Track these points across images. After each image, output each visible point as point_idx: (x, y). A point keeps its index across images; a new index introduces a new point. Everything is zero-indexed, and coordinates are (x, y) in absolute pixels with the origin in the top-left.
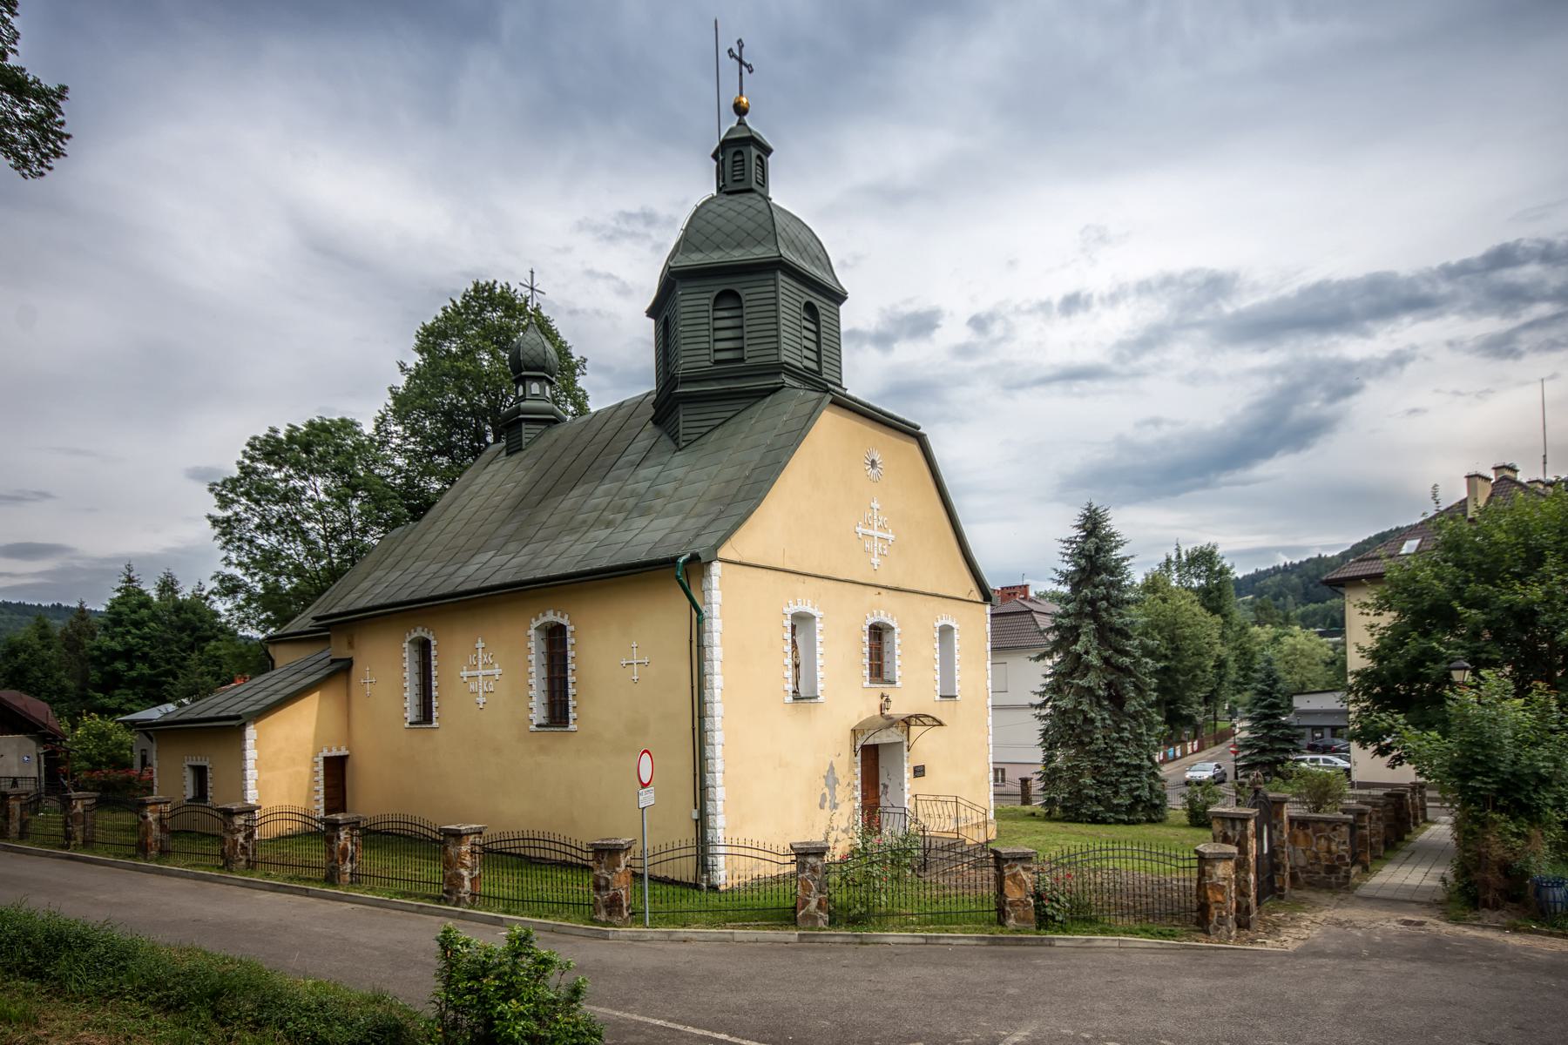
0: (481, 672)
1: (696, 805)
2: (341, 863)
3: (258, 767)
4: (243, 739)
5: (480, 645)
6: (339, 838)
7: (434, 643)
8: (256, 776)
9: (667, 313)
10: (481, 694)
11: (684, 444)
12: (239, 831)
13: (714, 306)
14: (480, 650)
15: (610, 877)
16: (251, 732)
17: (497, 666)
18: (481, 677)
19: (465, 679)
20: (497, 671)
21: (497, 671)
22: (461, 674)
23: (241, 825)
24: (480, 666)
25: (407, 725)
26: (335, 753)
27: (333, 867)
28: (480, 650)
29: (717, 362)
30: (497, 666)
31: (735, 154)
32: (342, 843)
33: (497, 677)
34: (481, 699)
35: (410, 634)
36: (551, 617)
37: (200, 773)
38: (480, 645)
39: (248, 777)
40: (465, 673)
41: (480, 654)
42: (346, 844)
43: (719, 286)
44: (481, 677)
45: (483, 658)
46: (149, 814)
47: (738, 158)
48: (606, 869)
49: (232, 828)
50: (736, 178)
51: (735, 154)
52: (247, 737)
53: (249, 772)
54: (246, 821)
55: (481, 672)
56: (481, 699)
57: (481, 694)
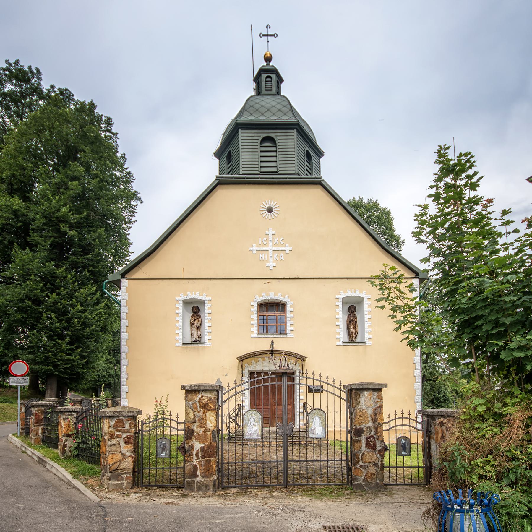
10: (271, 260)
13: (261, 144)
14: (271, 236)
18: (271, 251)
22: (251, 249)
24: (271, 244)
28: (271, 236)
29: (262, 173)
30: (287, 245)
31: (267, 77)
33: (287, 251)
43: (264, 133)
44: (271, 251)
47: (269, 79)
50: (267, 89)
51: (267, 77)
55: (271, 247)
57: (271, 260)
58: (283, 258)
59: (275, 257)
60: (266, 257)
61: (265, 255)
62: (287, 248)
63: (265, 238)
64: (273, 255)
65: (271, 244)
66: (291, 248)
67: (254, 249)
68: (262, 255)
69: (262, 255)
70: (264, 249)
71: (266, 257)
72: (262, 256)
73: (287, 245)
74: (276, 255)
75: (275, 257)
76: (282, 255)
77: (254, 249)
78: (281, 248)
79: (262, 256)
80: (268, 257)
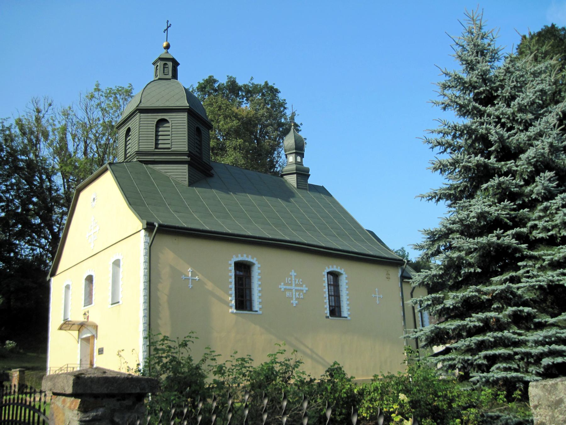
0: (293, 287)
5: (293, 273)
14: (293, 277)
18: (294, 290)
21: (305, 288)
28: (293, 277)
30: (304, 286)
33: (304, 291)
34: (294, 302)
41: (293, 280)
44: (294, 290)
45: (295, 281)
55: (293, 287)
56: (294, 302)
57: (294, 299)
58: (302, 297)
59: (297, 296)
62: (305, 288)
63: (289, 279)
64: (296, 295)
65: (294, 285)
66: (307, 289)
72: (288, 294)
74: (297, 293)
75: (297, 296)
76: (301, 294)
77: (282, 287)
78: (302, 288)
79: (288, 294)
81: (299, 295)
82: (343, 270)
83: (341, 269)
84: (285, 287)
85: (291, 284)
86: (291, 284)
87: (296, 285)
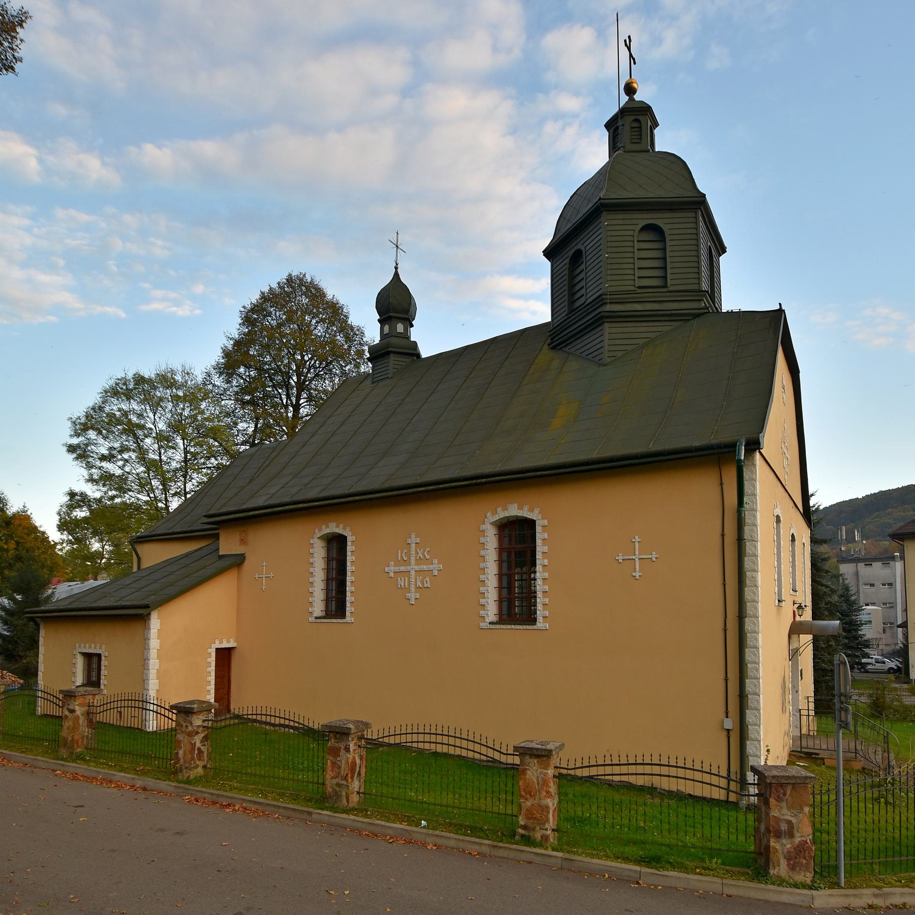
1: (727, 714)
2: (350, 780)
3: (159, 657)
4: (147, 628)
5: (414, 539)
6: (347, 749)
7: (349, 539)
8: (157, 667)
9: (579, 246)
10: (413, 588)
11: (609, 360)
12: (197, 733)
14: (413, 546)
15: (794, 820)
16: (155, 622)
17: (436, 561)
18: (413, 573)
19: (392, 575)
20: (436, 566)
21: (436, 566)
23: (198, 726)
24: (413, 561)
25: (311, 619)
26: (225, 645)
27: (338, 785)
28: (413, 546)
32: (350, 757)
34: (413, 595)
35: (320, 530)
36: (514, 510)
37: (92, 660)
38: (414, 539)
39: (151, 667)
40: (391, 569)
42: (354, 758)
44: (413, 573)
46: (77, 708)
48: (789, 808)
49: (190, 728)
52: (152, 626)
53: (151, 662)
54: (204, 721)
55: (414, 567)
57: (413, 588)
59: (419, 584)
60: (406, 584)
61: (405, 579)
67: (391, 569)
68: (401, 579)
69: (401, 579)
70: (402, 568)
71: (406, 584)
72: (401, 583)
73: (436, 561)
75: (419, 584)
80: (409, 582)
81: (422, 582)
82: (536, 511)
83: (521, 508)
84: (397, 569)
85: (407, 562)
86: (407, 562)
87: (419, 561)
